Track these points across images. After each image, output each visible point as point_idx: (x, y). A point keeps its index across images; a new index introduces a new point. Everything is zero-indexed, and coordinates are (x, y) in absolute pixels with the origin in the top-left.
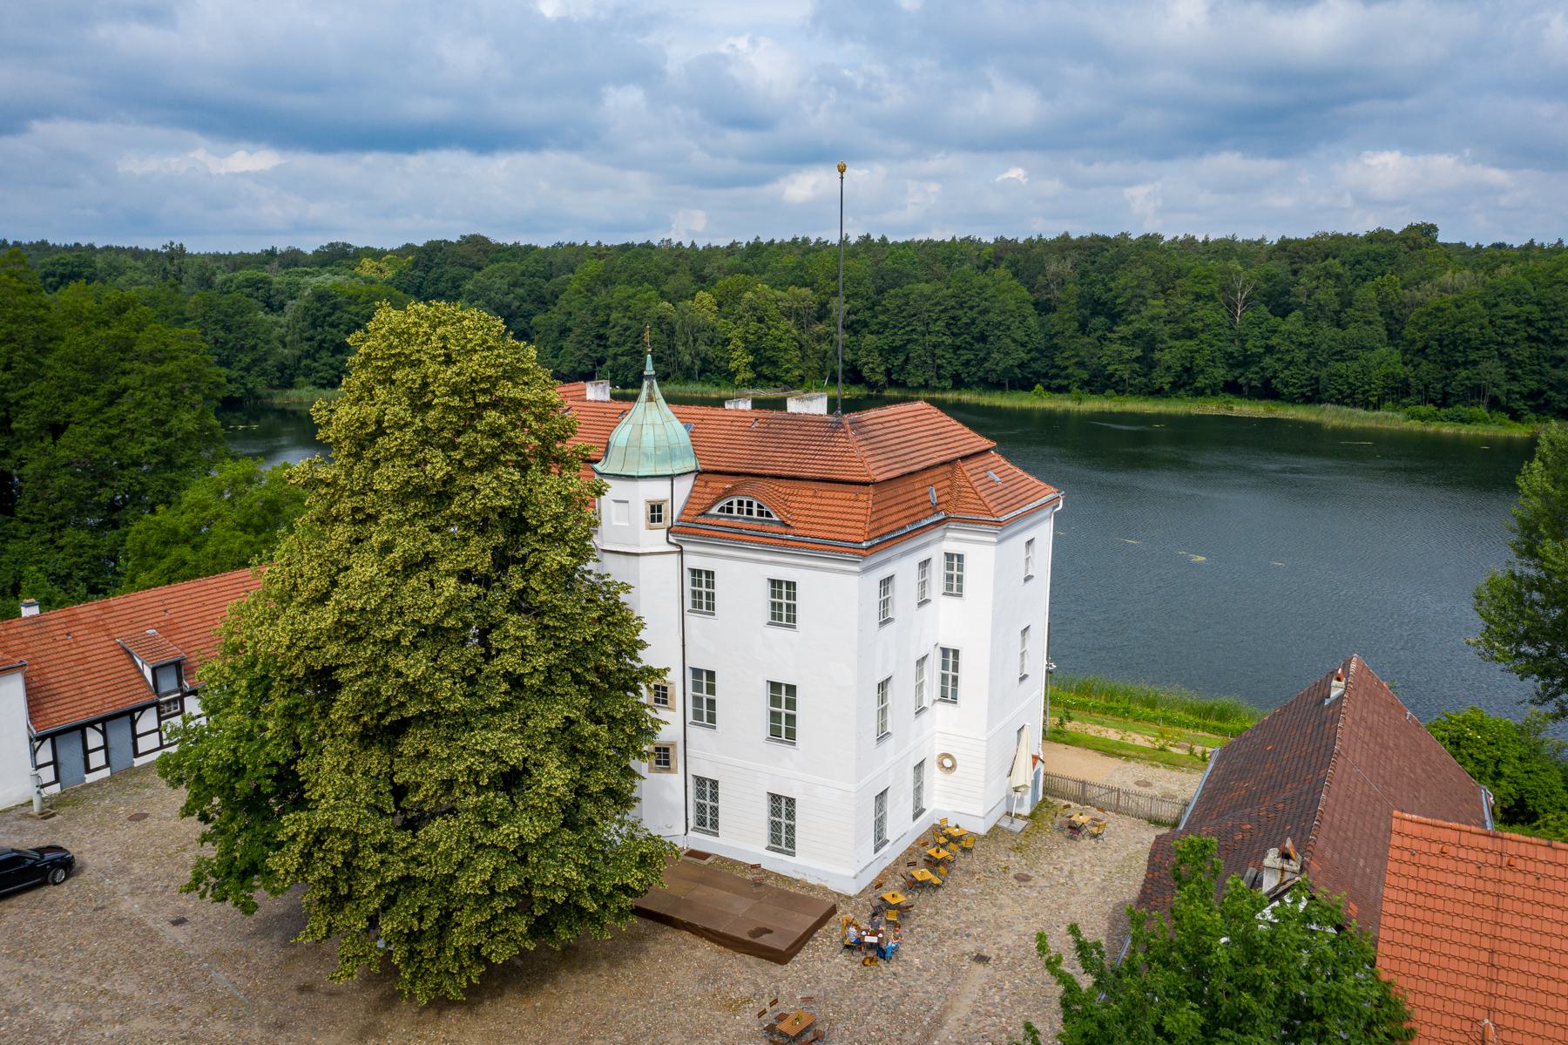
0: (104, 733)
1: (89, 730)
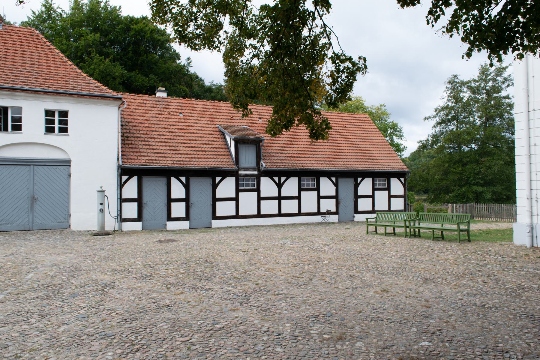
0: (187, 186)
1: (174, 180)
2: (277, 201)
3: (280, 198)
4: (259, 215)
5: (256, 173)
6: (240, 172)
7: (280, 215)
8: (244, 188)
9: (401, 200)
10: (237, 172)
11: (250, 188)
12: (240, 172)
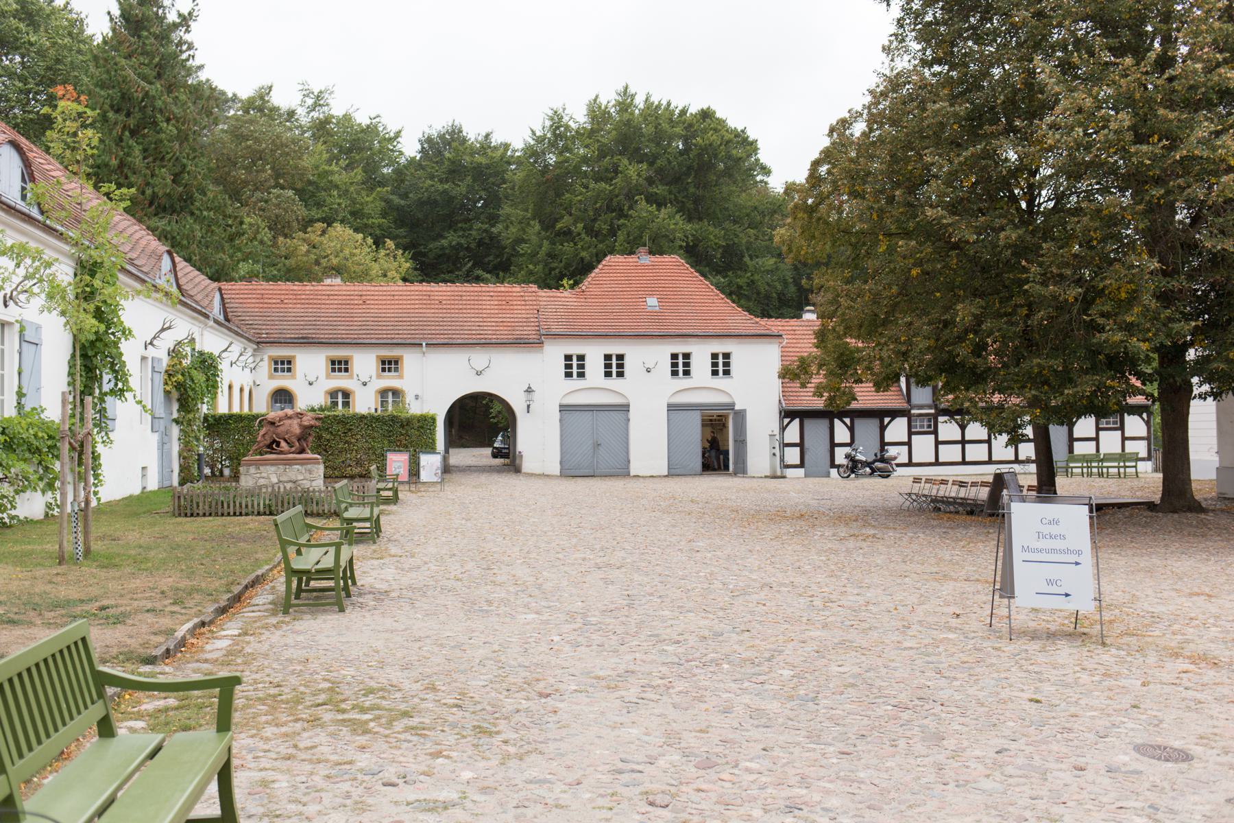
0: (851, 429)
1: (837, 422)
2: (960, 446)
3: (963, 442)
4: (937, 463)
5: (932, 411)
6: (913, 412)
7: (964, 462)
8: (918, 430)
9: (1144, 443)
10: (909, 411)
11: (925, 429)
12: (913, 412)
